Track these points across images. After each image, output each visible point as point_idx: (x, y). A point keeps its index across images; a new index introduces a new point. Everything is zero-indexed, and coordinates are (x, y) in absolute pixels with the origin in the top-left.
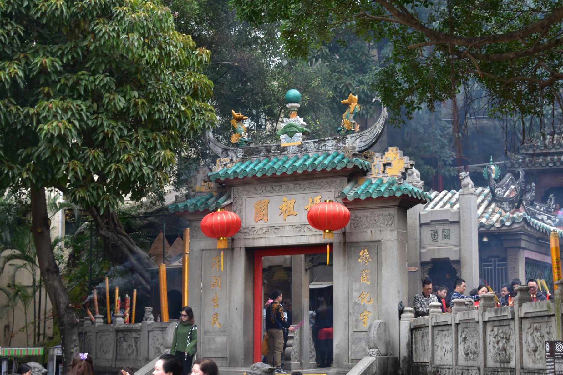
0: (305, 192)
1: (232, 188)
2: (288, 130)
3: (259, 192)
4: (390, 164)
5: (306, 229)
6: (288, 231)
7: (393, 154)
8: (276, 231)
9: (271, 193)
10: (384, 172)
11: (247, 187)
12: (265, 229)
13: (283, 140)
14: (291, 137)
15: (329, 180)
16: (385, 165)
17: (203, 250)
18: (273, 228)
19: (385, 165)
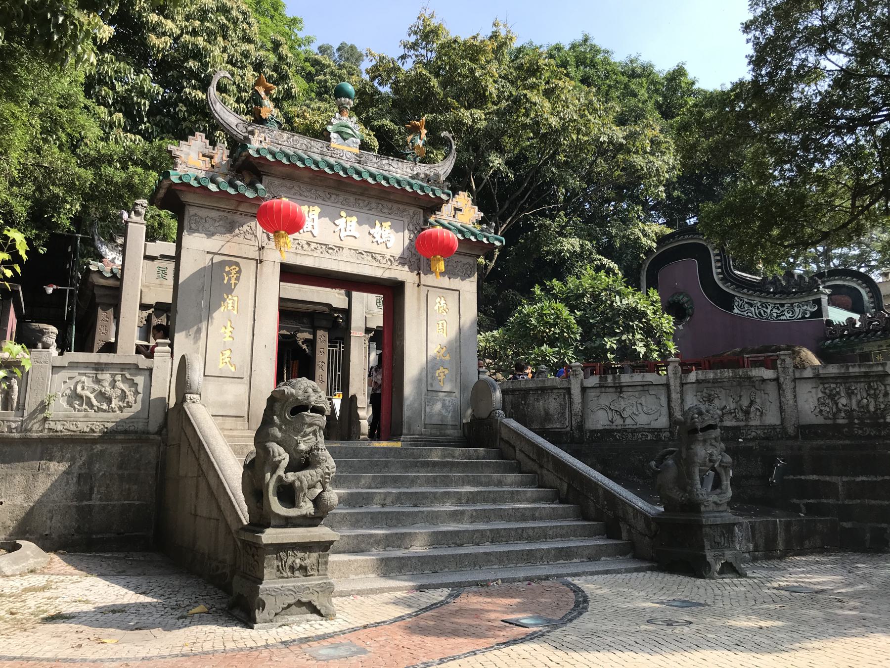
0: (370, 212)
1: (264, 177)
2: (345, 130)
3: (305, 194)
4: (460, 210)
5: (370, 258)
6: (345, 255)
7: (463, 199)
8: (330, 251)
9: (324, 200)
10: (454, 216)
11: (288, 183)
12: (313, 246)
13: (332, 140)
14: (345, 139)
15: (402, 207)
16: (456, 209)
17: (208, 252)
18: (324, 247)
19: (456, 209)
